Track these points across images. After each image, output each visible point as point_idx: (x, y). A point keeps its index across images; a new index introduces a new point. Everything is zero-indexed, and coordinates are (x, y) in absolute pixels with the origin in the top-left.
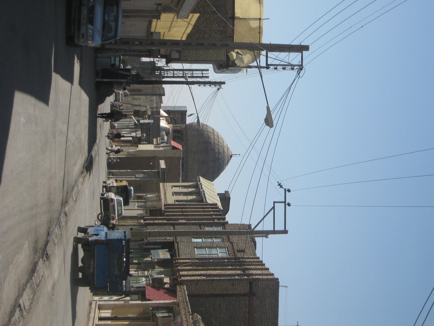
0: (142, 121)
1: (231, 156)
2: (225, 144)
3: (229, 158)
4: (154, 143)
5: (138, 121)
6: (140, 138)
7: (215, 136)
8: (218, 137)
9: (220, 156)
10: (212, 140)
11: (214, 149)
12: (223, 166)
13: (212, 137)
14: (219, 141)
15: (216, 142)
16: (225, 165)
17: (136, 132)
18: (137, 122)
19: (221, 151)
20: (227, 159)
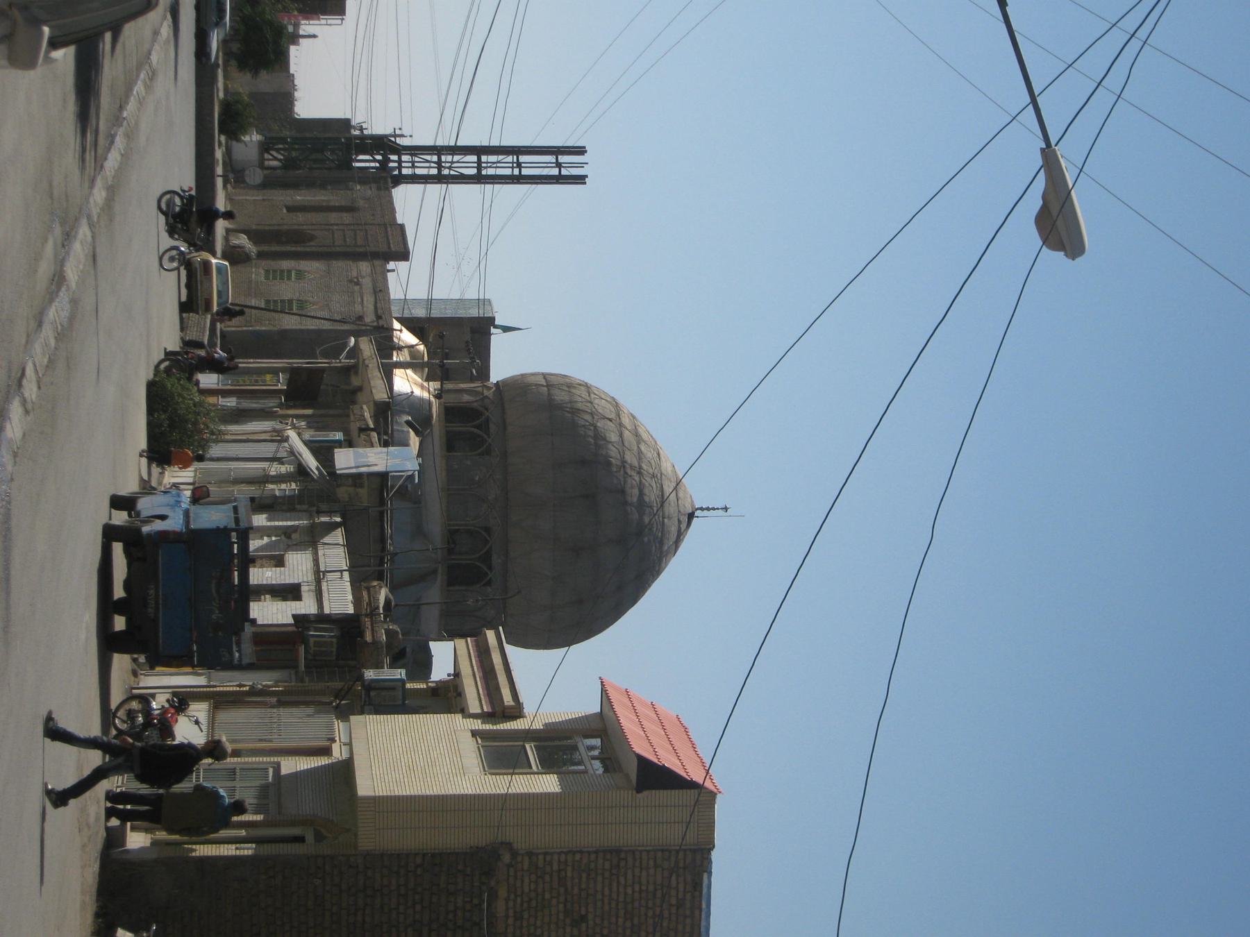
0: (345, 460)
1: (691, 516)
2: (666, 466)
3: (683, 526)
4: (474, 708)
5: (324, 452)
6: (348, 627)
7: (626, 434)
8: (637, 435)
9: (646, 520)
10: (613, 452)
11: (623, 492)
12: (660, 560)
13: (614, 437)
14: (640, 452)
15: (629, 457)
16: (668, 552)
17: (311, 539)
18: (311, 462)
19: (651, 496)
20: (674, 529)
